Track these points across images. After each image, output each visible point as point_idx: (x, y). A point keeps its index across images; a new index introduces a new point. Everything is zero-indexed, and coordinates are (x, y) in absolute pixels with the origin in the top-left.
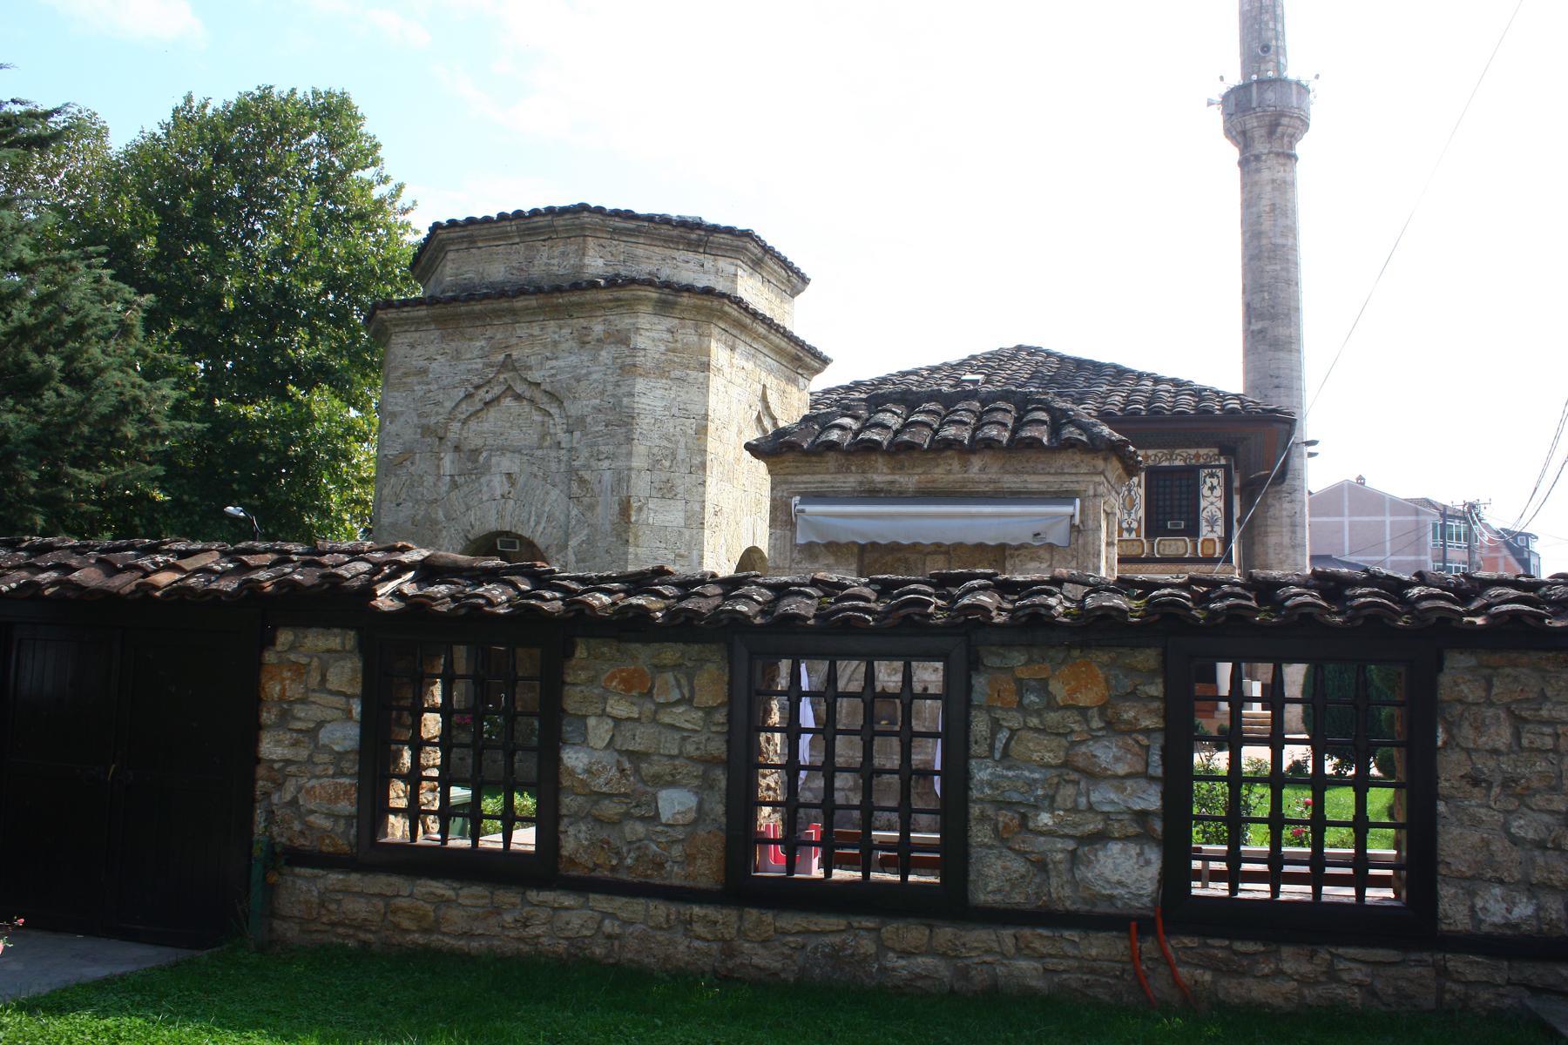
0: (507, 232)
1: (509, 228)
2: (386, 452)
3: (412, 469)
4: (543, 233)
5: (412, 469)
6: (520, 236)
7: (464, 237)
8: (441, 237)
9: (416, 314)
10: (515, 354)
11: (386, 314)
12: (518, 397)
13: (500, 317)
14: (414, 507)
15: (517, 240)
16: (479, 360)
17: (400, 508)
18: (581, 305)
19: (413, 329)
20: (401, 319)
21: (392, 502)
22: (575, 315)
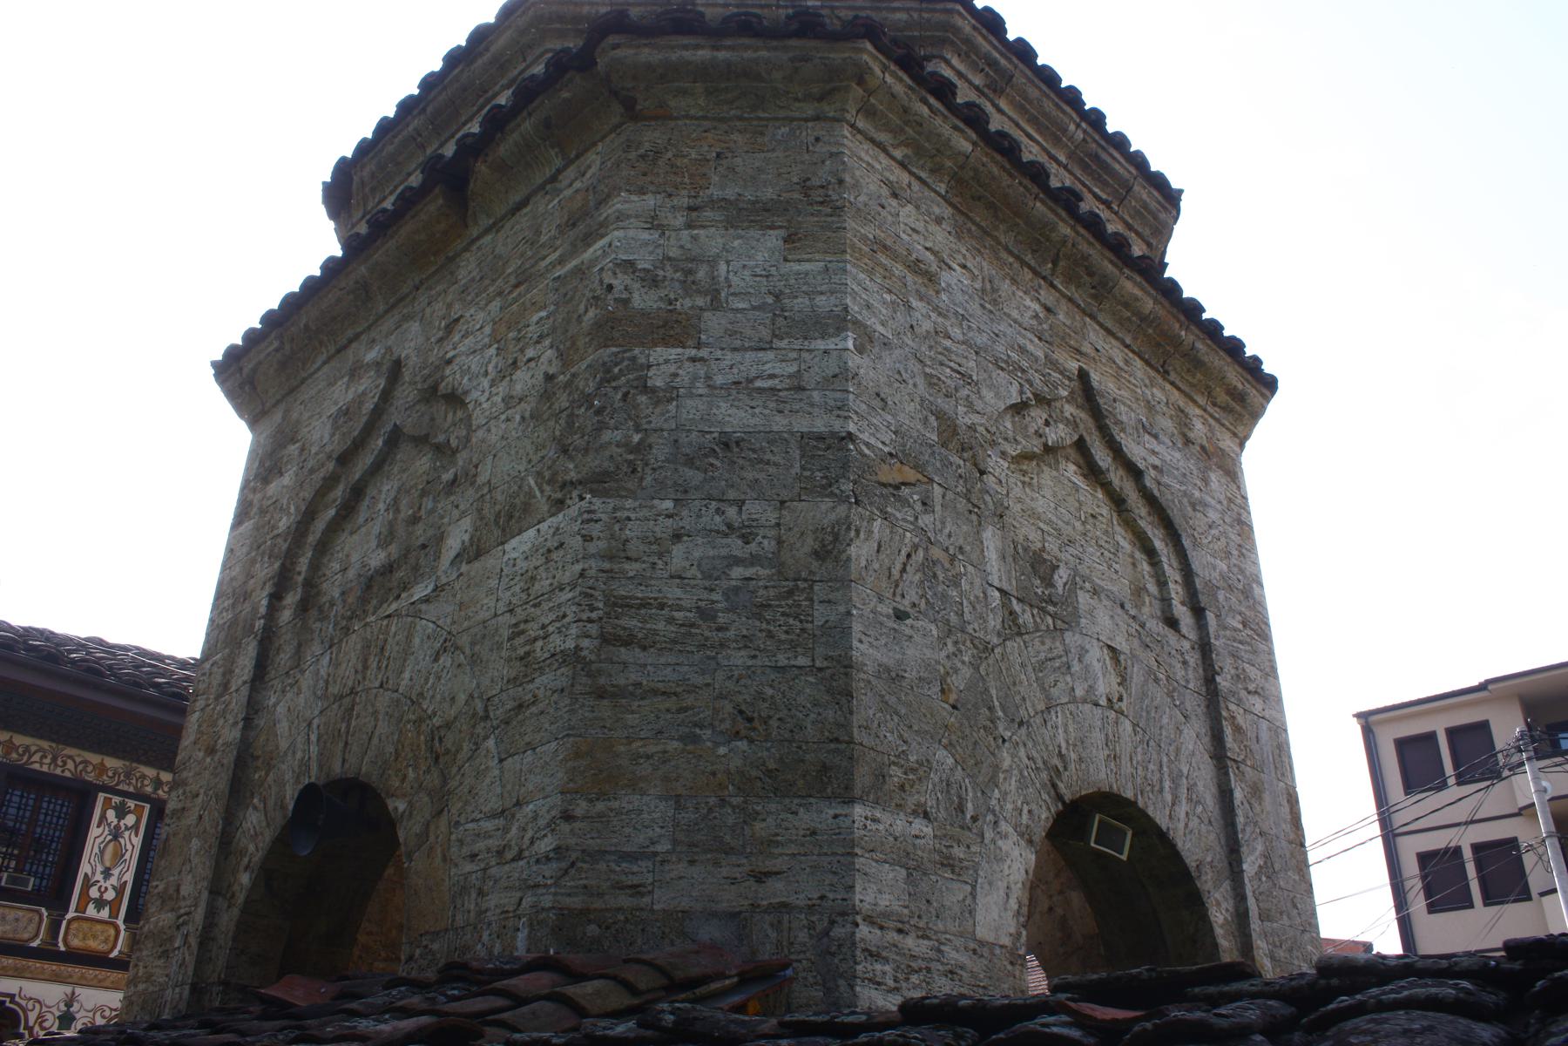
0: (1064, 131)
1: (1072, 127)
2: (852, 428)
3: (926, 520)
4: (1104, 184)
5: (926, 520)
6: (1069, 157)
7: (993, 64)
8: (959, 22)
9: (946, 130)
10: (1095, 377)
11: (885, 69)
12: (1092, 472)
13: (1070, 279)
14: (942, 641)
15: (1062, 158)
16: (1036, 340)
17: (905, 627)
18: (1197, 364)
19: (898, 154)
20: (906, 110)
21: (881, 600)
22: (1173, 376)
